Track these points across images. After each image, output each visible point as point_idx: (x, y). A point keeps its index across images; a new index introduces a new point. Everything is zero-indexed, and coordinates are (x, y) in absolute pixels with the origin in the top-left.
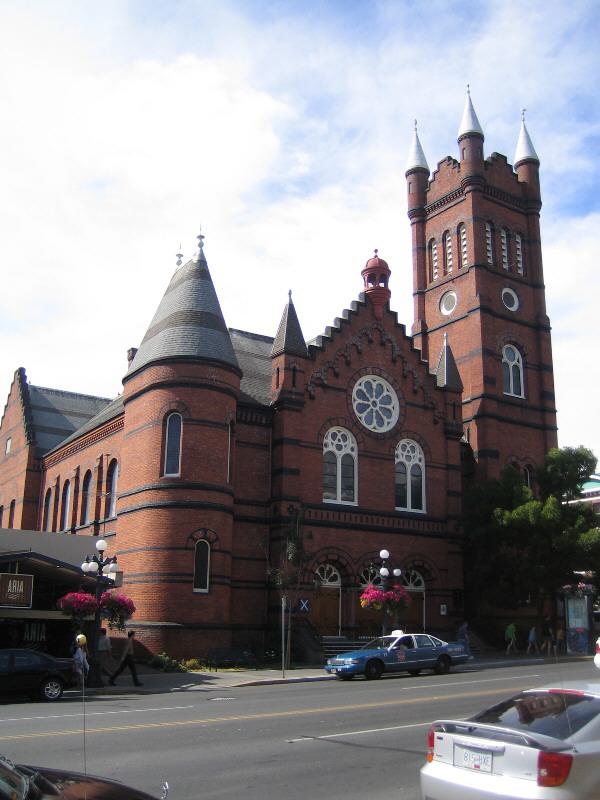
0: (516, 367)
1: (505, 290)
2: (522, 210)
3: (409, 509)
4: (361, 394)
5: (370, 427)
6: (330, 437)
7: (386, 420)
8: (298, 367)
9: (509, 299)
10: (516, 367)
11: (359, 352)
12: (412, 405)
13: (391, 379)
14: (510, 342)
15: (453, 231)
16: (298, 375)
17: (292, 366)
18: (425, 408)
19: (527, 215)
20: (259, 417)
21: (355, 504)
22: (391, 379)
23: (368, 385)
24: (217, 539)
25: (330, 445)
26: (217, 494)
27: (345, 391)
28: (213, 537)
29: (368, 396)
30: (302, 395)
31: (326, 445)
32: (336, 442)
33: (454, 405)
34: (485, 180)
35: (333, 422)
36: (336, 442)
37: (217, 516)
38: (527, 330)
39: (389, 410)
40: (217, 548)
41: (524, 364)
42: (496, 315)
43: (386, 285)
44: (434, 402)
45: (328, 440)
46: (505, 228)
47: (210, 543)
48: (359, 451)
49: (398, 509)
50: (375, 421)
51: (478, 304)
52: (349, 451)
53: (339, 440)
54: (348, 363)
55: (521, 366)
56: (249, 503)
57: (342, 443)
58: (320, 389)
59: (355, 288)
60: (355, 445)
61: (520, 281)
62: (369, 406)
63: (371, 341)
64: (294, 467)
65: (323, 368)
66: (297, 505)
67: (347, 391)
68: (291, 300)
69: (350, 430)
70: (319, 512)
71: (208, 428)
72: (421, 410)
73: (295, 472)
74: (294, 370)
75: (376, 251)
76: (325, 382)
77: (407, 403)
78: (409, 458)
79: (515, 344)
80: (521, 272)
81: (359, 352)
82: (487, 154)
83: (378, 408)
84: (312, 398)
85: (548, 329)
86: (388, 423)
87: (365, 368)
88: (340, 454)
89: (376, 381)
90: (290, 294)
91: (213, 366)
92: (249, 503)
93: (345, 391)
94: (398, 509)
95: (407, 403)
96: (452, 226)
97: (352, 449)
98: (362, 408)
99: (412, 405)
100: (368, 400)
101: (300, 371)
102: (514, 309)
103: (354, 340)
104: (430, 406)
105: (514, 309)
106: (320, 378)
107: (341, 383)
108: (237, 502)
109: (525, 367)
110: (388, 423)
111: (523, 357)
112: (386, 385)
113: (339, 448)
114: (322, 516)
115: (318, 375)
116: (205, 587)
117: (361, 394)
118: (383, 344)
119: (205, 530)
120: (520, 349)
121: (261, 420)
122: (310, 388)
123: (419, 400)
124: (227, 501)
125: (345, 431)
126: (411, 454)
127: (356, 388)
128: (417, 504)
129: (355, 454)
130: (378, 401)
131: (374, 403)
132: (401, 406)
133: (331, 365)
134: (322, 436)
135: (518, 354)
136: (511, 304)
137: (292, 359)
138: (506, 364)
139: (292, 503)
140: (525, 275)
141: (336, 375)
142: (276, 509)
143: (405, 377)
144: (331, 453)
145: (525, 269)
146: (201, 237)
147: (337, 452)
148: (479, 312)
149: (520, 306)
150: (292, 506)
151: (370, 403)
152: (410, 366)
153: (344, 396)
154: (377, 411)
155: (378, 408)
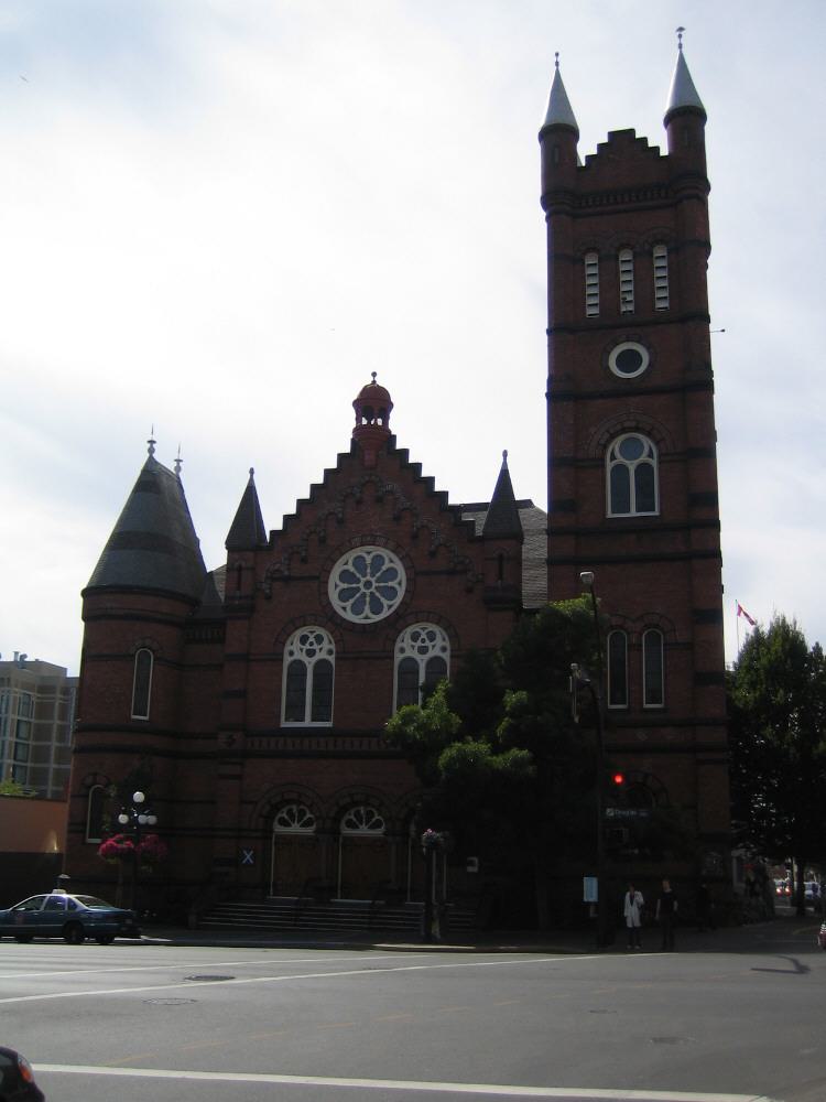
6: (297, 644)
8: (243, 564)
10: (644, 469)
14: (624, 430)
18: (451, 573)
25: (295, 650)
27: (318, 578)
39: (393, 588)
53: (311, 644)
54: (322, 541)
59: (335, 436)
60: (333, 647)
75: (374, 374)
81: (341, 522)
82: (586, 148)
87: (349, 541)
88: (310, 663)
111: (657, 443)
112: (386, 553)
118: (379, 500)
120: (649, 434)
122: (264, 586)
125: (320, 631)
131: (368, 584)
134: (280, 642)
135: (647, 442)
141: (304, 560)
143: (415, 537)
146: (152, 442)
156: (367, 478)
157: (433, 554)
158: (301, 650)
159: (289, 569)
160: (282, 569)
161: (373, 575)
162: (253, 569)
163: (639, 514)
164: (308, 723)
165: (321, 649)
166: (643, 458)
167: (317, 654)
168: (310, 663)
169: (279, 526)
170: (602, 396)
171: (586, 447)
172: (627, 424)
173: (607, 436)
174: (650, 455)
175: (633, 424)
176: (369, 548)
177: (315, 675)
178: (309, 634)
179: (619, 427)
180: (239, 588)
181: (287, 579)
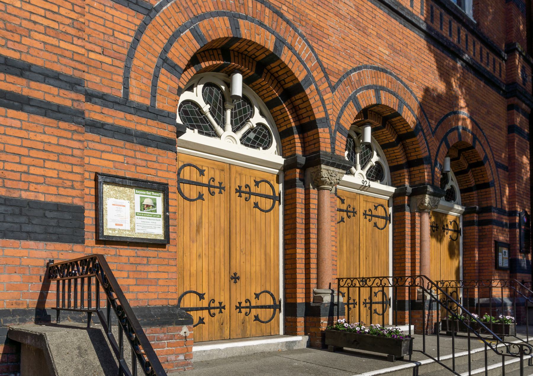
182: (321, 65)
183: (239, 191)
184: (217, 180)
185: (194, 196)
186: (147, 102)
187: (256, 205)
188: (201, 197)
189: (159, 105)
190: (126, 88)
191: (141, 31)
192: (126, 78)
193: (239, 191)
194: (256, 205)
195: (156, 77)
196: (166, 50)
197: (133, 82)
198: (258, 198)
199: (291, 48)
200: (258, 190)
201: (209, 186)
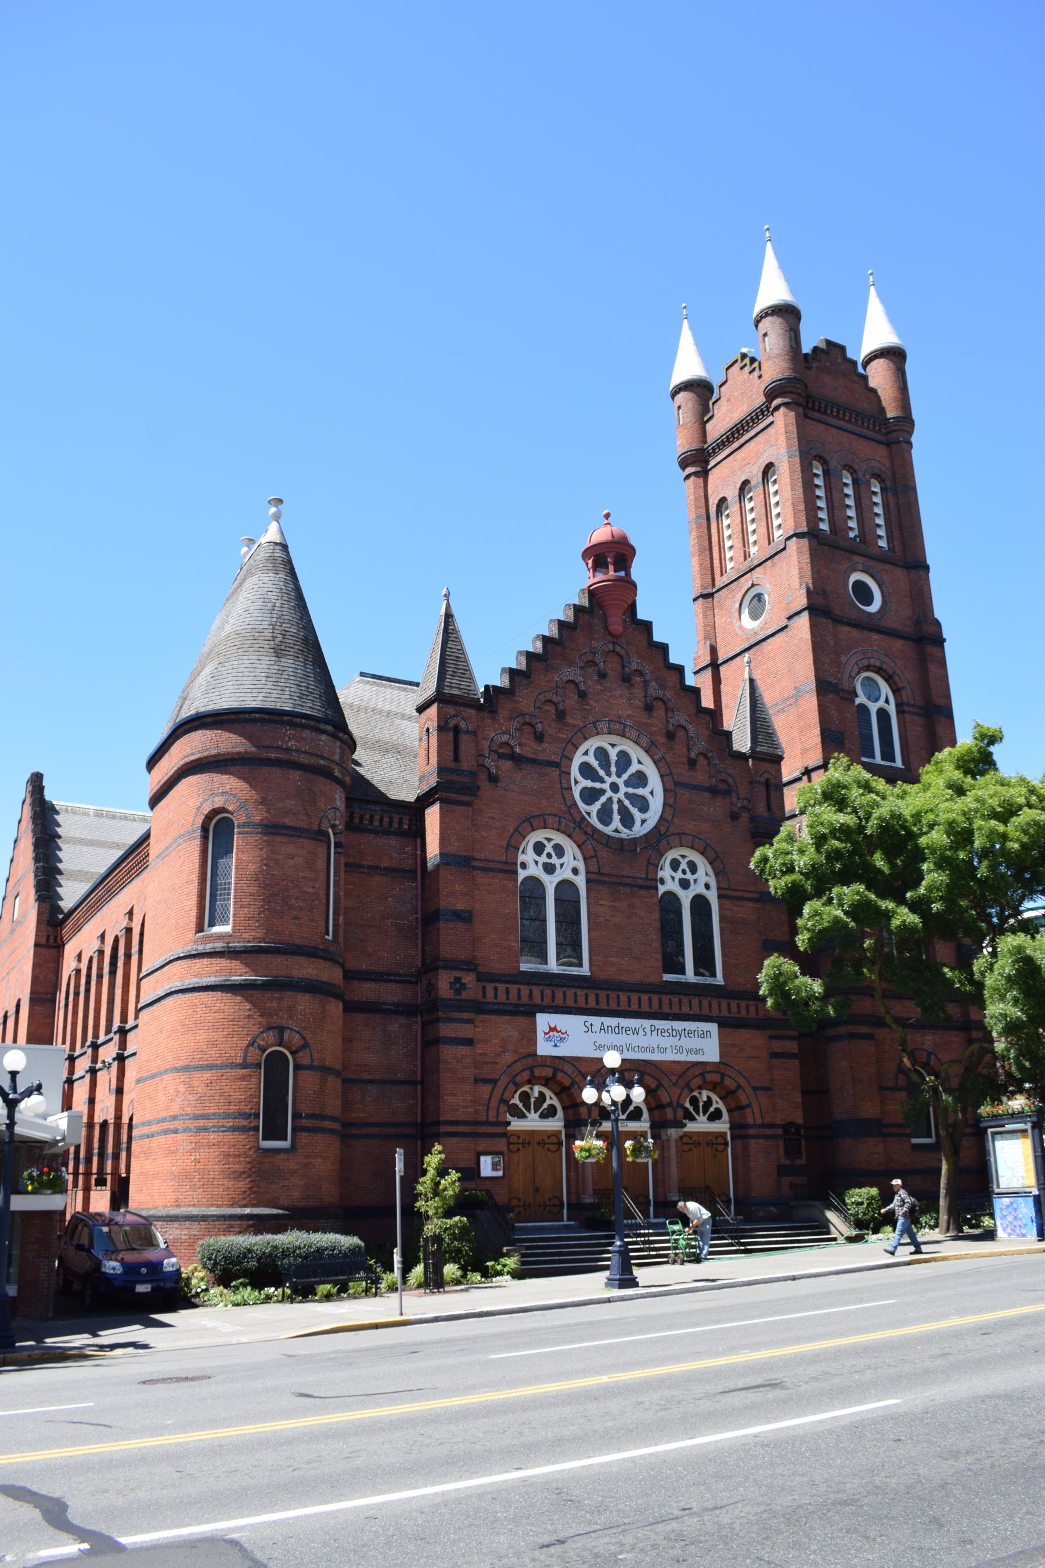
0: (883, 714)
1: (855, 577)
2: (878, 437)
3: (690, 975)
4: (586, 770)
5: (608, 830)
6: (530, 849)
7: (638, 815)
8: (463, 725)
9: (863, 593)
10: (883, 714)
11: (582, 695)
12: (685, 786)
13: (644, 741)
14: (868, 668)
15: (756, 479)
16: (464, 738)
17: (452, 723)
18: (714, 791)
19: (888, 445)
20: (396, 820)
21: (585, 970)
22: (644, 741)
23: (601, 754)
24: (305, 1046)
26: (303, 960)
27: (557, 765)
28: (296, 1040)
29: (602, 773)
30: (472, 774)
31: (524, 866)
32: (543, 859)
33: (767, 784)
34: (806, 386)
35: (533, 822)
36: (543, 859)
37: (304, 1003)
38: (899, 644)
39: (643, 798)
40: (306, 1062)
41: (898, 705)
42: (838, 621)
43: (628, 574)
44: (731, 781)
45: (528, 856)
46: (849, 468)
47: (292, 1053)
48: (587, 873)
49: (668, 977)
50: (616, 817)
51: (802, 601)
52: (568, 875)
54: (561, 715)
55: (892, 709)
56: (379, 977)
57: (554, 860)
58: (507, 765)
60: (581, 865)
61: (881, 558)
62: (603, 792)
63: (602, 675)
64: (460, 906)
65: (514, 725)
66: (469, 979)
67: (561, 767)
68: (448, 606)
69: (569, 836)
70: (513, 988)
71: (284, 839)
72: (707, 795)
73: (464, 917)
74: (456, 730)
76: (518, 750)
77: (676, 784)
78: (685, 884)
79: (879, 670)
80: (883, 543)
81: (582, 695)
82: (806, 348)
83: (621, 795)
84: (493, 779)
85: (940, 641)
86: (643, 822)
87: (594, 723)
88: (550, 883)
89: (615, 746)
90: (447, 596)
91: (294, 725)
92: (379, 977)
93: (557, 765)
94: (668, 977)
95: (676, 784)
96: (754, 473)
97: (575, 871)
98: (591, 796)
99: (685, 786)
100: (602, 781)
101: (468, 732)
102: (874, 607)
103: (570, 673)
104: (722, 786)
105: (874, 607)
106: (507, 744)
107: (548, 751)
108: (350, 975)
109: (899, 712)
110: (643, 822)
111: (894, 692)
112: (635, 752)
113: (549, 869)
114: (519, 998)
115: (505, 738)
116: (286, 1139)
117: (586, 770)
118: (626, 680)
119: (281, 1030)
120: (889, 679)
121: (400, 823)
122: (488, 762)
123: (700, 776)
124: (332, 974)
126: (689, 876)
127: (578, 760)
128: (569, 946)
129: (580, 881)
130: (620, 782)
131: (615, 787)
132: (666, 790)
133: (528, 719)
134: (513, 848)
135: (885, 688)
136: (868, 600)
137: (451, 710)
138: (864, 710)
139: (457, 974)
140: (891, 548)
141: (539, 738)
142: (432, 988)
143: (670, 736)
144: (533, 880)
145: (890, 538)
147: (545, 878)
148: (805, 615)
149: (884, 601)
150: (458, 980)
151: (606, 786)
152: (681, 718)
153: (555, 773)
154: (620, 801)
155: (621, 795)
156: (611, 647)
157: (692, 763)
158: (536, 862)
159: (520, 744)
160: (512, 743)
161: (619, 775)
162: (474, 733)
163: (883, 763)
164: (553, 965)
165: (562, 865)
166: (881, 703)
167: (558, 870)
168: (550, 883)
169: (498, 680)
170: (848, 624)
171: (840, 676)
172: (873, 662)
173: (856, 669)
174: (887, 701)
175: (878, 664)
176: (614, 739)
177: (557, 900)
178: (545, 842)
179: (866, 663)
180: (456, 758)
181: (518, 760)
182: (580, 1072)
183: (539, 1144)
184: (527, 1139)
185: (515, 1149)
186: (495, 1120)
187: (548, 1150)
188: (518, 1149)
189: (500, 1120)
190: (487, 1115)
191: (492, 1091)
192: (487, 1112)
193: (539, 1144)
194: (548, 1150)
195: (498, 1108)
196: (502, 1095)
197: (490, 1113)
198: (550, 1146)
199: (562, 1071)
200: (550, 1141)
201: (522, 1144)
